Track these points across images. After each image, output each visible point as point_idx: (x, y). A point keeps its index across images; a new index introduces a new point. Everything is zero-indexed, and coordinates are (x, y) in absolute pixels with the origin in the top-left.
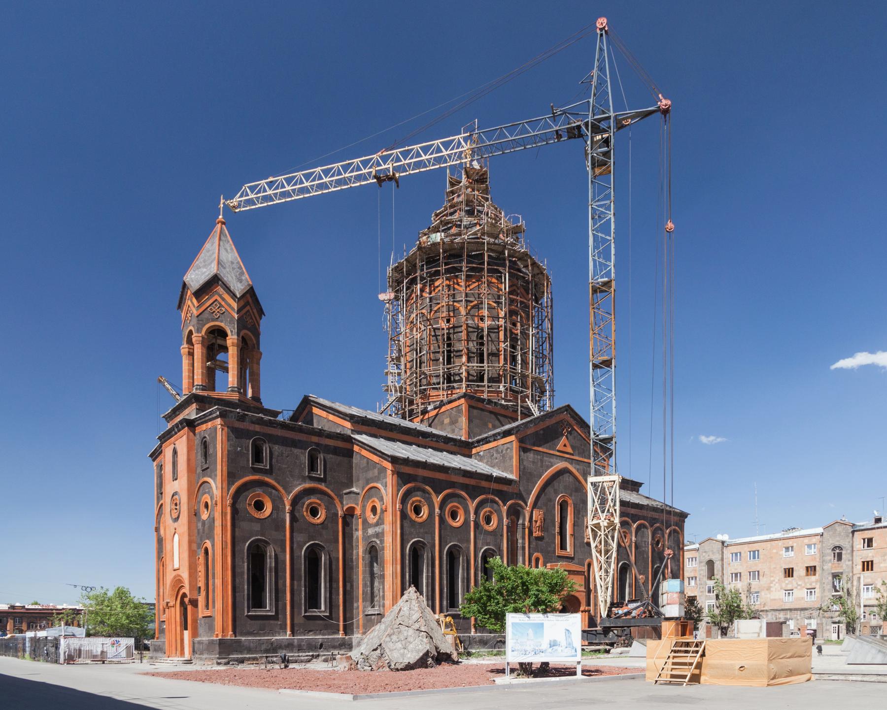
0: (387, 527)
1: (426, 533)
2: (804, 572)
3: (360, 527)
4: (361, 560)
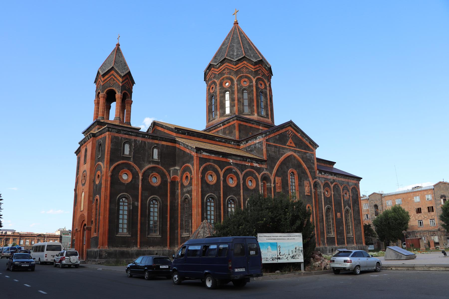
0: (194, 187)
2: (427, 210)
3: (179, 188)
4: (179, 206)
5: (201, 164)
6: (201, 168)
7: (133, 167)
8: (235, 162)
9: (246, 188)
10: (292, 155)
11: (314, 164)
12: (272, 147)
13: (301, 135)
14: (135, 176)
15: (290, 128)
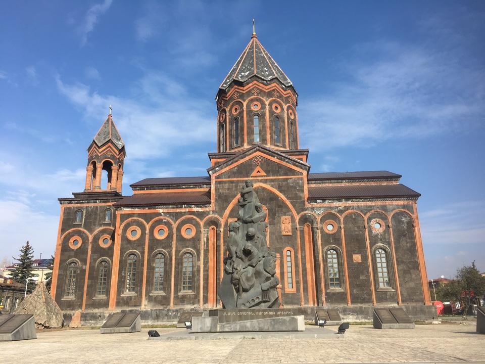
1: (139, 246)
5: (122, 221)
6: (123, 225)
7: (84, 232)
8: (166, 211)
9: (181, 239)
10: (260, 186)
11: (303, 191)
12: (226, 183)
13: (277, 158)
14: (85, 240)
15: (258, 153)
